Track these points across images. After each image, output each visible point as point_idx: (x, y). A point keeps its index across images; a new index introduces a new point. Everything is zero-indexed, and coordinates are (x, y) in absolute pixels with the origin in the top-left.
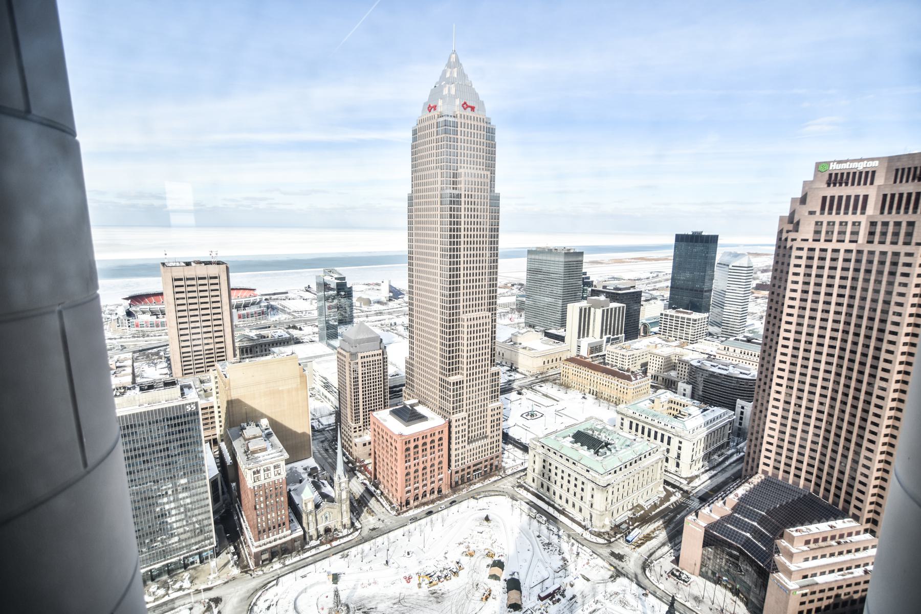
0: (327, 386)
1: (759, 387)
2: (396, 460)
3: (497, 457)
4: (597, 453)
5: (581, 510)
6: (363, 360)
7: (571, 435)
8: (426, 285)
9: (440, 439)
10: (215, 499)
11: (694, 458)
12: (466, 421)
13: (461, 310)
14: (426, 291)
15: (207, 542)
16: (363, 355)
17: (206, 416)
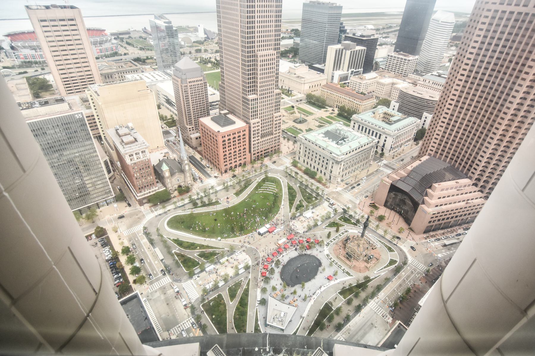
0: (168, 101)
1: (439, 105)
2: (217, 147)
3: (278, 145)
4: (337, 143)
5: (325, 174)
6: (190, 84)
7: (323, 132)
8: (230, 29)
9: (244, 135)
10: (109, 172)
11: (393, 146)
13: (256, 49)
14: (231, 33)
15: (109, 195)
16: (190, 80)
17: (90, 122)
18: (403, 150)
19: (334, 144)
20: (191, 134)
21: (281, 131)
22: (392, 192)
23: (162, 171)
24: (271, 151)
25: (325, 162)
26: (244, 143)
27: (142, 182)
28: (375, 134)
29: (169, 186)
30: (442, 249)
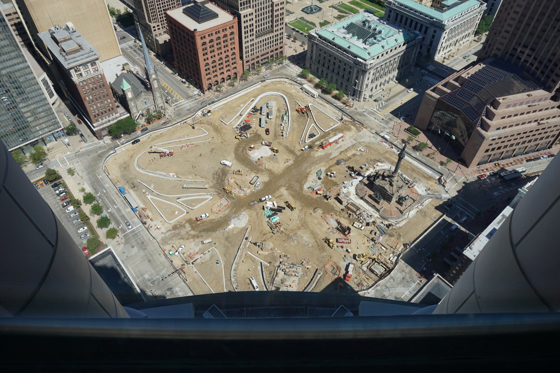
3: (281, 48)
4: (365, 42)
7: (345, 26)
9: (232, 33)
10: (51, 95)
12: (254, 16)
15: (56, 126)
18: (458, 50)
19: (360, 43)
20: (156, 35)
21: (284, 26)
22: (439, 110)
23: (123, 91)
24: (272, 56)
25: (347, 71)
26: (233, 46)
27: (98, 108)
28: (419, 26)
29: (134, 110)
30: (500, 186)
